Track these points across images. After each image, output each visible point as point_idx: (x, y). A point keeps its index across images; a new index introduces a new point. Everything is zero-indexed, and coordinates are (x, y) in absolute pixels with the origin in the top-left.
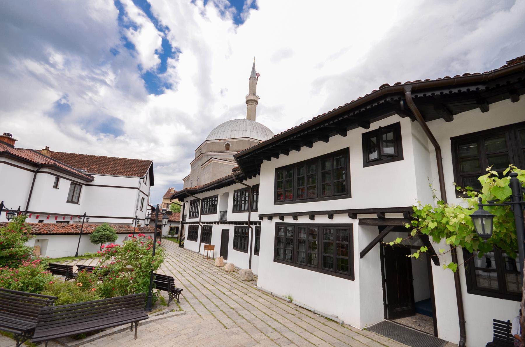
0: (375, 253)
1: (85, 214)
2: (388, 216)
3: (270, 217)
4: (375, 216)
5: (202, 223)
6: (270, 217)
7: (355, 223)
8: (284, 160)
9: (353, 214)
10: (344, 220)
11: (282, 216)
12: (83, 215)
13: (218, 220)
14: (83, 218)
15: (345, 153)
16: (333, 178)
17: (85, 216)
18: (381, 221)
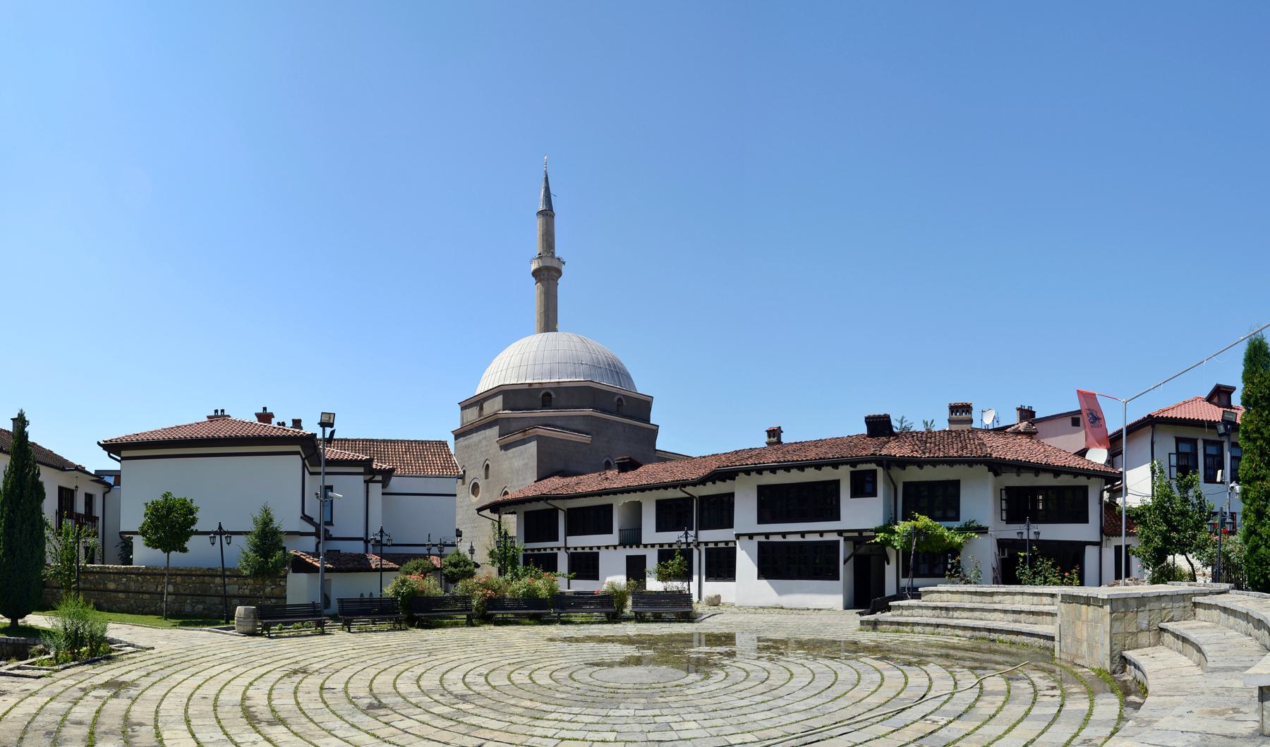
0: (851, 561)
1: (220, 527)
2: (865, 534)
3: (751, 536)
4: (856, 534)
7: (841, 539)
8: (768, 479)
9: (840, 533)
10: (834, 537)
11: (767, 535)
12: (216, 529)
14: (218, 537)
15: (837, 483)
16: (822, 502)
17: (221, 532)
18: (858, 539)
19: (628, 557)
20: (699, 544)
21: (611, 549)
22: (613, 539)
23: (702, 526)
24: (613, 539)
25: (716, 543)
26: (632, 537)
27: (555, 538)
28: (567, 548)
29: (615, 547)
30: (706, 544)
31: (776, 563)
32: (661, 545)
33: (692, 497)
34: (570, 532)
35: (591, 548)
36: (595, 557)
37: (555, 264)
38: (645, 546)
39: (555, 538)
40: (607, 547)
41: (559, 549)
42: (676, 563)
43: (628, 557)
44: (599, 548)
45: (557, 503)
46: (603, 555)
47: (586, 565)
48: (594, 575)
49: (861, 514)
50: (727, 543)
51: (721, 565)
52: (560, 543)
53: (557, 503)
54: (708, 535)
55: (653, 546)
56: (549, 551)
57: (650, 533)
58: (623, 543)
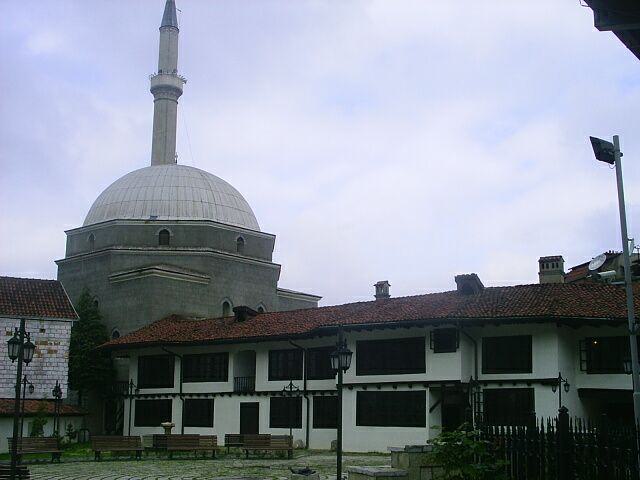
0: (439, 407)
5: (184, 395)
6: (351, 386)
13: (232, 390)
18: (442, 389)
19: (242, 404)
20: (306, 392)
21: (226, 398)
22: (228, 386)
23: (309, 377)
24: (228, 386)
25: (323, 392)
26: (246, 387)
27: (172, 386)
28: (182, 395)
29: (230, 394)
30: (314, 392)
31: (375, 410)
32: (273, 393)
33: (300, 350)
34: (185, 378)
35: (206, 395)
36: (211, 403)
37: (175, 83)
38: (259, 394)
39: (172, 386)
40: (222, 394)
41: (174, 395)
42: (286, 411)
43: (242, 404)
44: (214, 395)
45: (174, 350)
46: (218, 402)
47: (200, 411)
48: (208, 422)
49: (445, 367)
50: (332, 392)
51: (328, 414)
52: (175, 390)
53: (174, 350)
54: (314, 385)
55: (266, 393)
56: (163, 398)
57: (263, 382)
58: (237, 392)
